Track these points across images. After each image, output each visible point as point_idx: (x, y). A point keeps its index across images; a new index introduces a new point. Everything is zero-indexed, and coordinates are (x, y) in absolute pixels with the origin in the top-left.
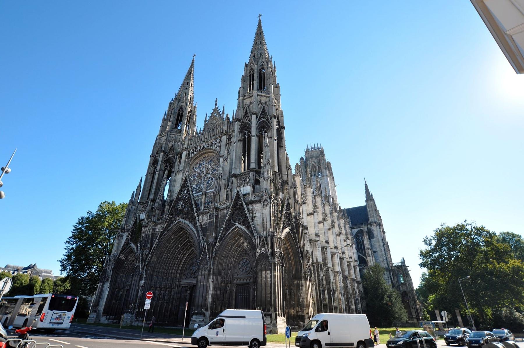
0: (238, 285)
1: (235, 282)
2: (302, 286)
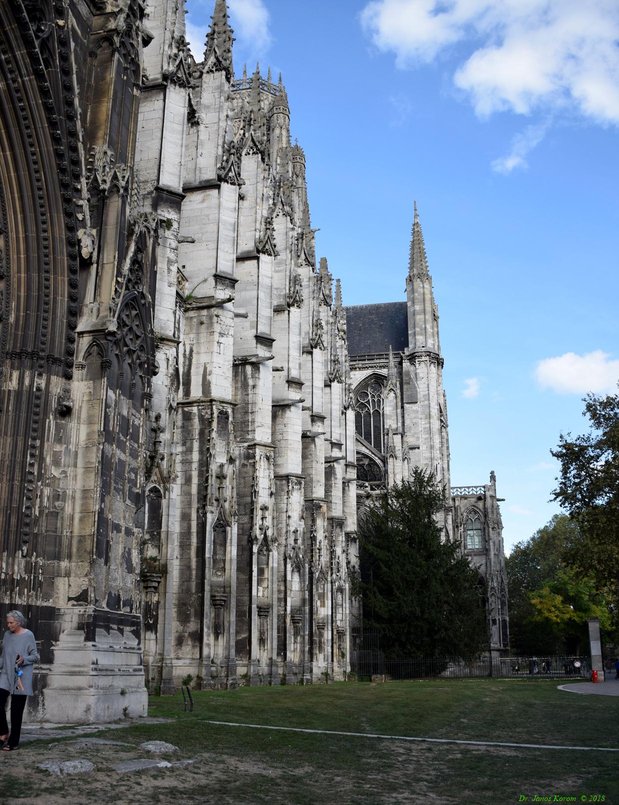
2: (65, 412)
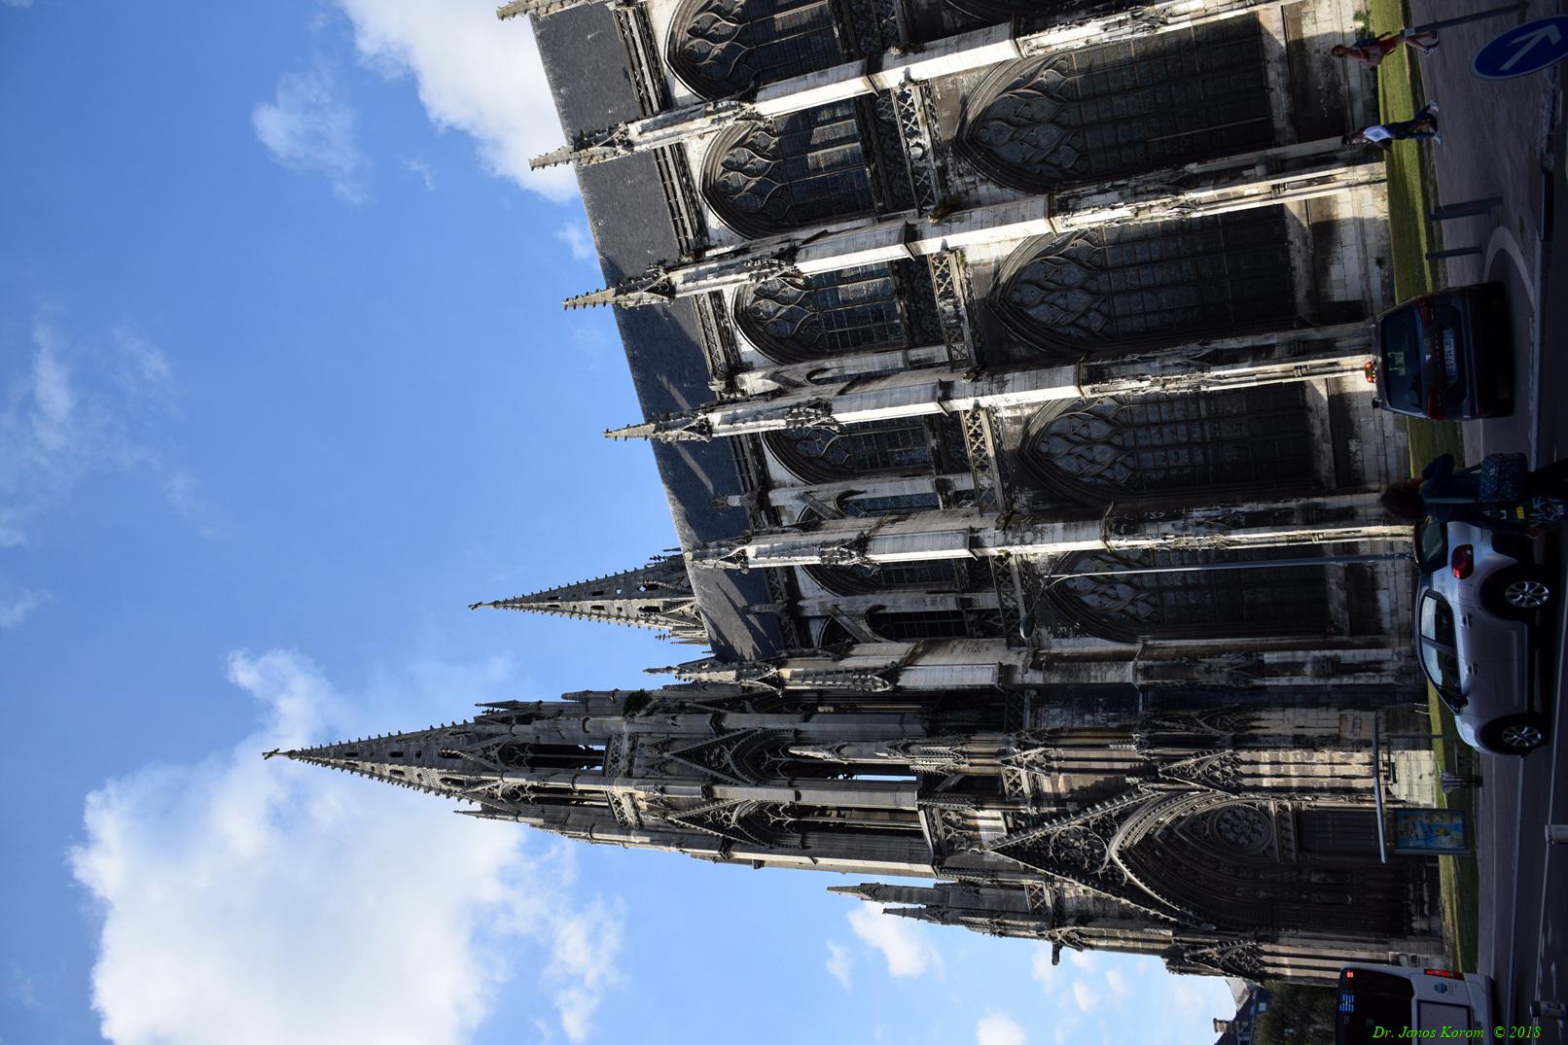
0: (1301, 847)
1: (1293, 856)
